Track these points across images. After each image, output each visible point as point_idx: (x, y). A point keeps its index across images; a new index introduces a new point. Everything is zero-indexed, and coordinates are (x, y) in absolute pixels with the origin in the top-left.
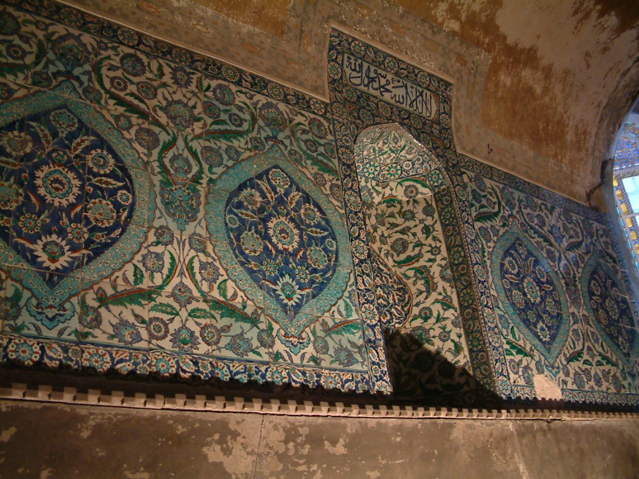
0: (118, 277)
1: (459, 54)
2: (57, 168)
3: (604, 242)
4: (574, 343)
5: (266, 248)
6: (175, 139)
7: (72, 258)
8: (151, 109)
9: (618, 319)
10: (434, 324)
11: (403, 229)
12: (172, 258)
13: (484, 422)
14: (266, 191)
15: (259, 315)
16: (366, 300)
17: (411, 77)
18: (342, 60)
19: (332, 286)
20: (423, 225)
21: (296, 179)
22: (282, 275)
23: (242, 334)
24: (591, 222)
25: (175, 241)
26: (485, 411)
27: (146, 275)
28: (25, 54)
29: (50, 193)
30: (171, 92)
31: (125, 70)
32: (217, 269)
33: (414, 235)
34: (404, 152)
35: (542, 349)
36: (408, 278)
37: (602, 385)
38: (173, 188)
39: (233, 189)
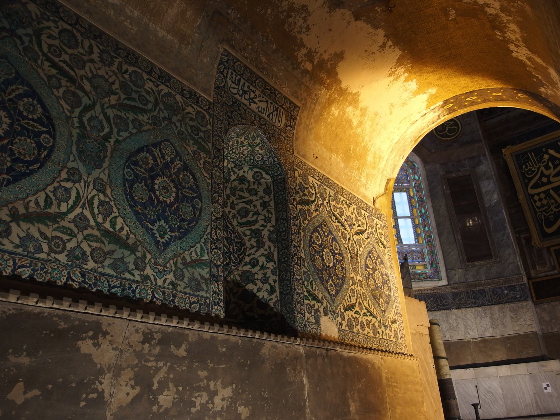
0: (31, 201)
1: (307, 87)
3: (380, 233)
4: (350, 298)
5: (151, 198)
6: (94, 104)
8: (78, 77)
9: (381, 286)
10: (259, 271)
12: (78, 193)
13: (284, 344)
14: (157, 157)
15: (138, 246)
18: (227, 74)
20: (262, 201)
22: (159, 220)
23: (123, 258)
24: (374, 218)
25: (82, 181)
26: (286, 338)
27: (55, 202)
30: (97, 68)
31: (61, 41)
34: (258, 147)
36: (246, 235)
37: (365, 329)
38: (87, 141)
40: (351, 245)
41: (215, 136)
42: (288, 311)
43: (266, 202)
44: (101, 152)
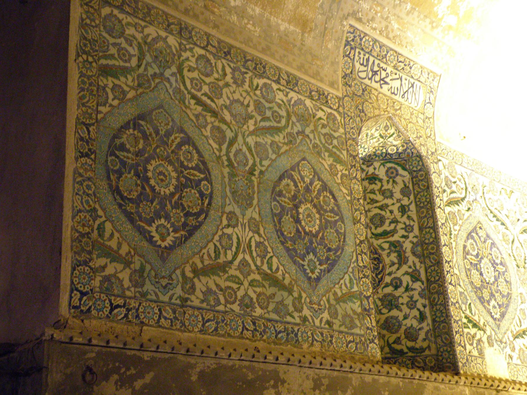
0: (204, 254)
2: (161, 162)
4: (520, 322)
5: (298, 231)
6: (236, 136)
7: (175, 237)
8: (219, 108)
10: (403, 293)
11: (382, 206)
14: (297, 181)
15: (293, 287)
16: (364, 275)
17: (407, 70)
18: (354, 55)
19: (341, 262)
20: (399, 205)
21: (318, 170)
22: (308, 253)
23: (282, 301)
25: (239, 224)
27: (222, 251)
28: (131, 56)
29: (158, 184)
30: (232, 92)
32: (266, 248)
33: (391, 212)
34: (392, 138)
35: (493, 326)
36: (383, 249)
38: (237, 179)
39: (275, 180)
40: (516, 249)
41: (349, 140)
42: (443, 342)
43: (405, 205)
44: (250, 189)
